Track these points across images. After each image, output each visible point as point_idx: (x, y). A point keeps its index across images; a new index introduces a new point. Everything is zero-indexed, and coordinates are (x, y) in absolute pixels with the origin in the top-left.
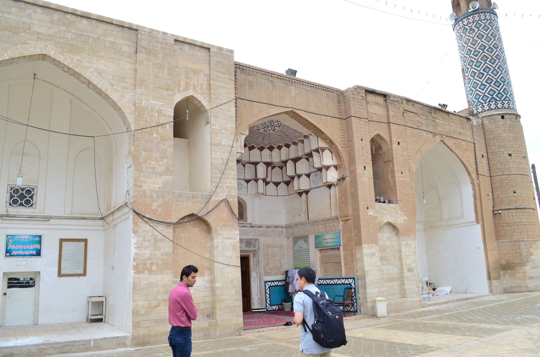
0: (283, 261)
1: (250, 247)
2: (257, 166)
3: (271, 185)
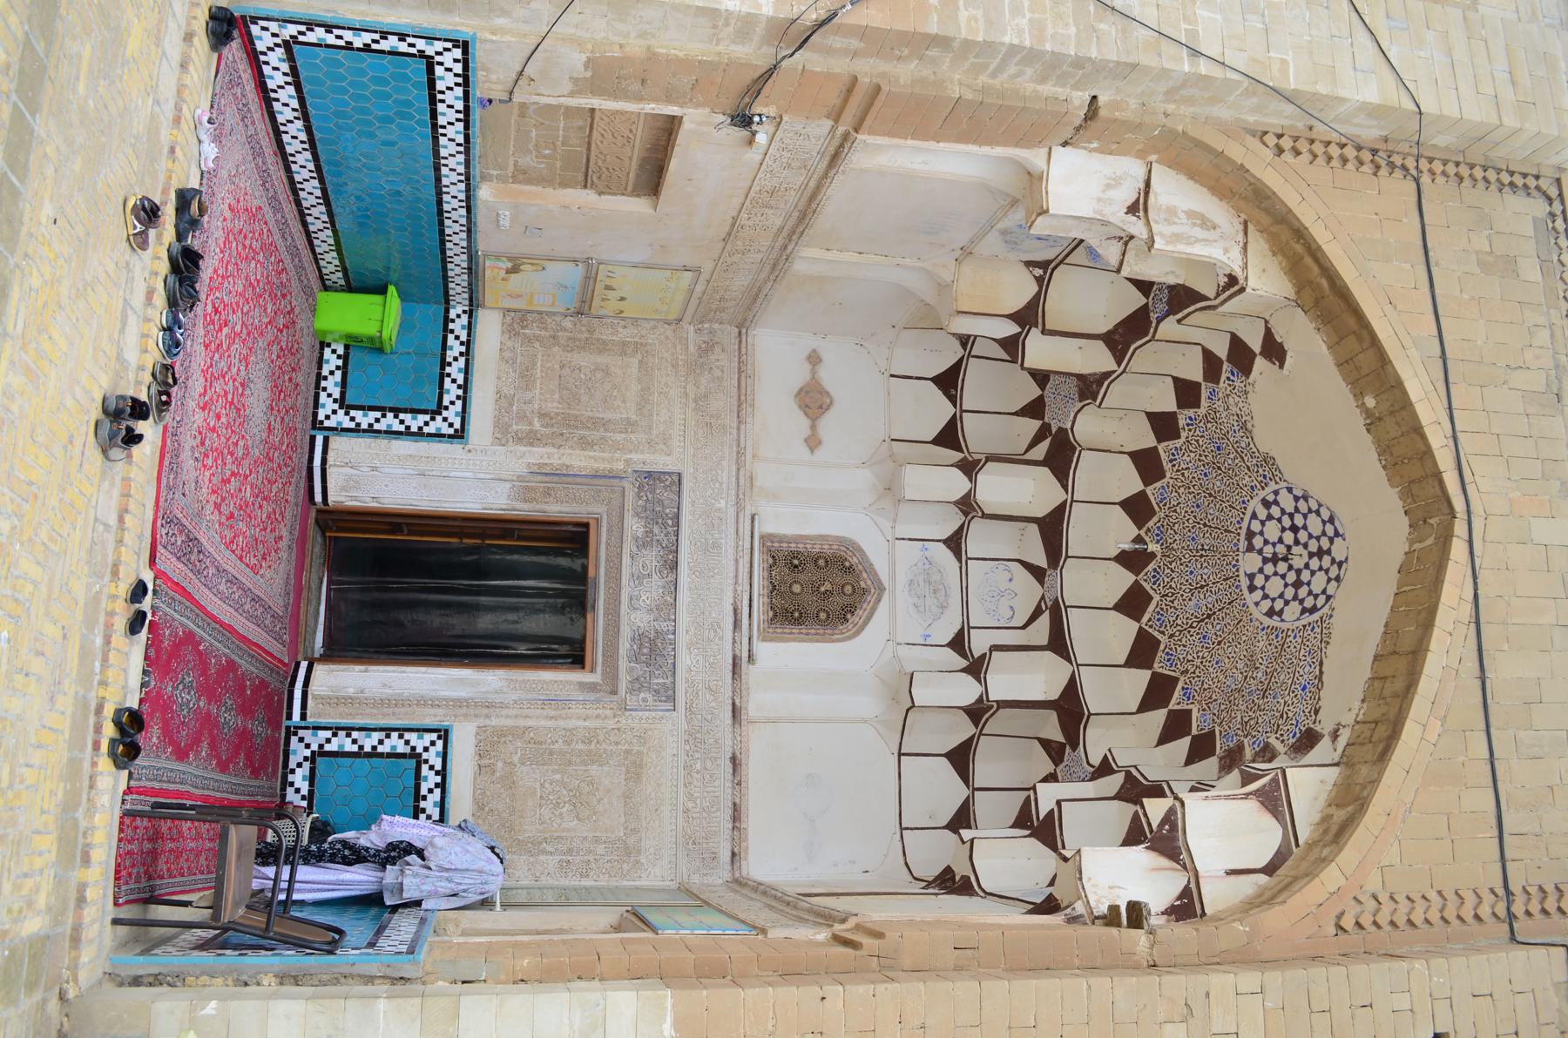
0: (551, 862)
1: (635, 657)
2: (1048, 654)
3: (966, 729)
